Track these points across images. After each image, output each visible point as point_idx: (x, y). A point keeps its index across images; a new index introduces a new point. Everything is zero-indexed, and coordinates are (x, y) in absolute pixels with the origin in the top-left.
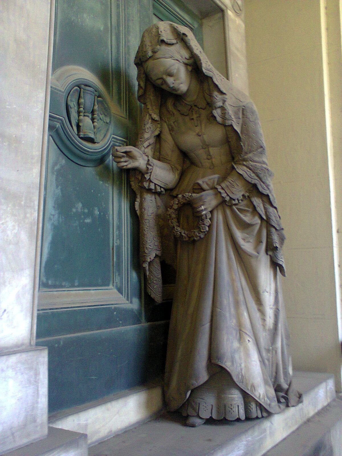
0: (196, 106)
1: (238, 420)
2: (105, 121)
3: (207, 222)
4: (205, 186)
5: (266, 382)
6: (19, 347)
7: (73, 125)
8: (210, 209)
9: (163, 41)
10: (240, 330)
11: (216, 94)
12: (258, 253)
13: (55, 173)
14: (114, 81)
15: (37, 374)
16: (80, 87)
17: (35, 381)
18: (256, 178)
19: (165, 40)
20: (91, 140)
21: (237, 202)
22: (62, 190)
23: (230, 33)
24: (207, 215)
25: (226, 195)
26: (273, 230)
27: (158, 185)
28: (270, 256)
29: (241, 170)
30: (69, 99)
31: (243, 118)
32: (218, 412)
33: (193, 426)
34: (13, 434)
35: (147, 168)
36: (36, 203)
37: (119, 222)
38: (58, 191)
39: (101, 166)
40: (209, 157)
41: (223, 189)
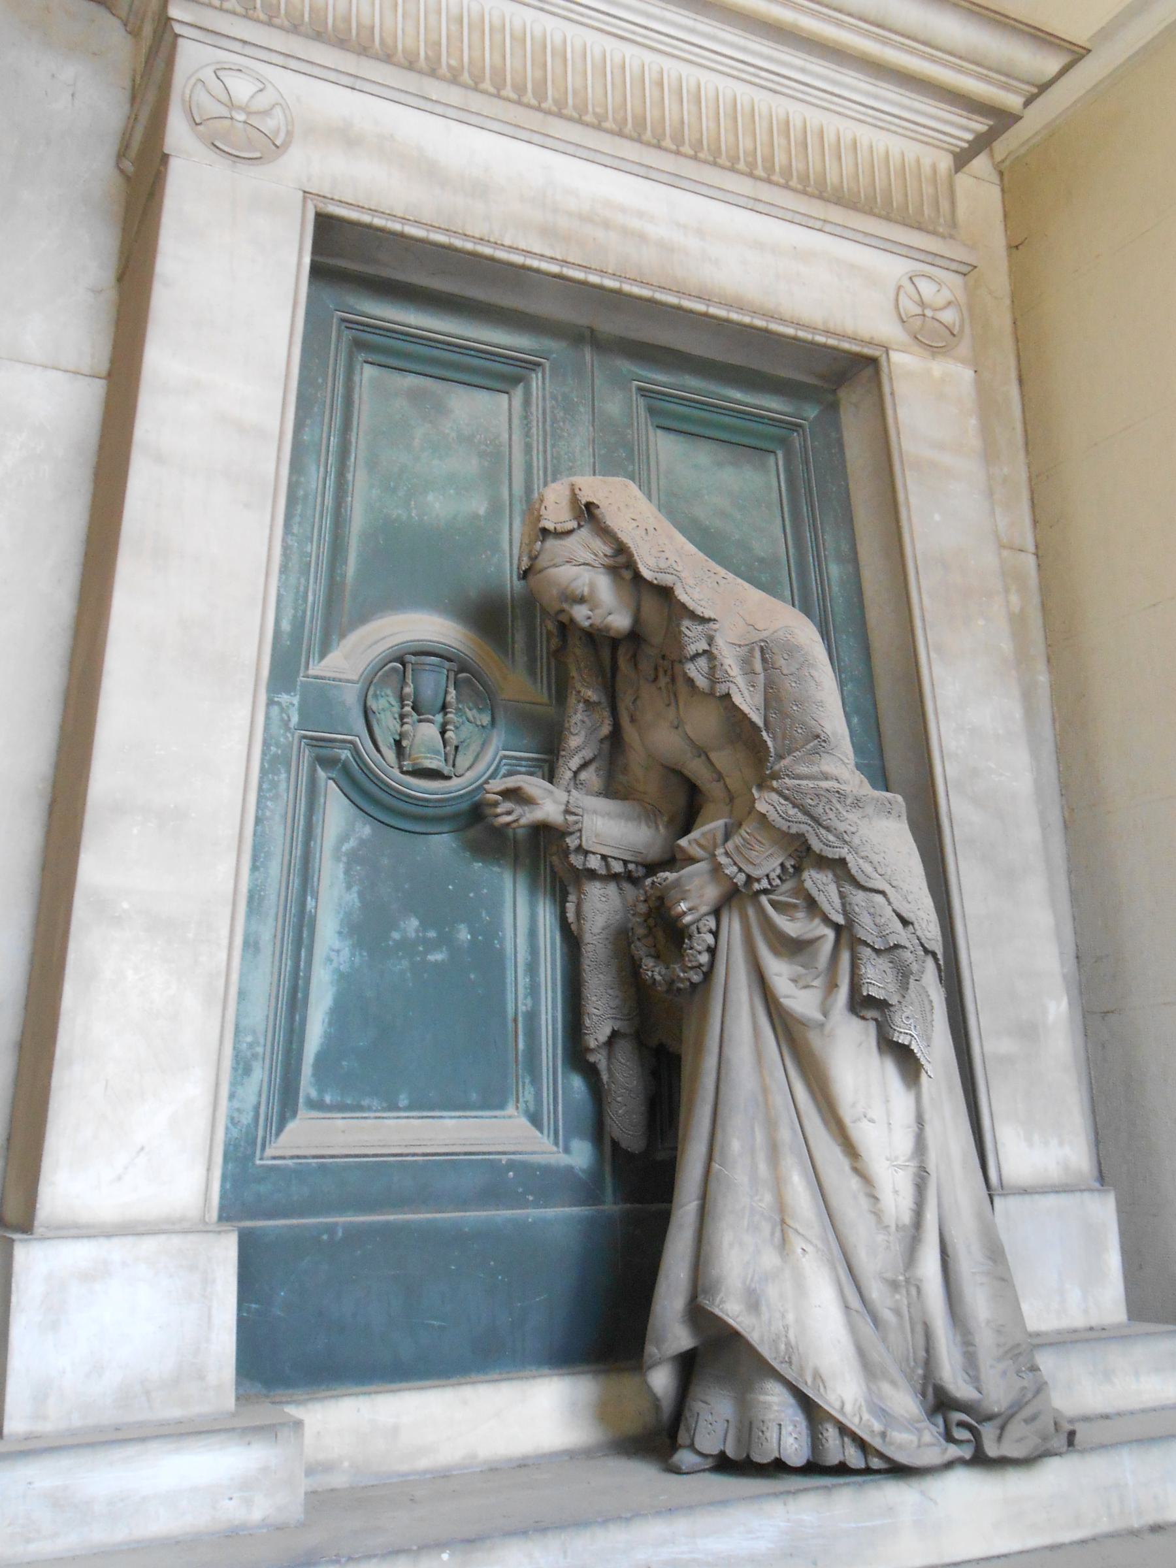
1: (779, 1468)
2: (479, 723)
4: (696, 851)
5: (869, 1369)
6: (173, 1223)
7: (383, 749)
8: (704, 909)
9: (545, 532)
10: (783, 1222)
11: (686, 623)
13: (344, 859)
14: (519, 623)
16: (404, 662)
19: (550, 526)
22: (361, 894)
23: (902, 413)
24: (701, 924)
25: (735, 869)
28: (876, 1020)
29: (765, 803)
30: (371, 693)
31: (765, 670)
32: (739, 1441)
33: (676, 1471)
34: (147, 1393)
36: (225, 932)
38: (353, 897)
39: (479, 827)
41: (727, 854)
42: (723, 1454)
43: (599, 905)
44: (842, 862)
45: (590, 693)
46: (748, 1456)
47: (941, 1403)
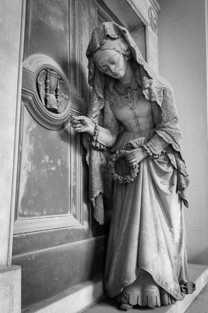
0: (129, 88)
3: (136, 171)
4: (135, 145)
8: (138, 162)
10: (158, 245)
12: (171, 192)
13: (29, 134)
15: (12, 288)
17: (11, 294)
18: (172, 140)
20: (55, 111)
21: (157, 156)
25: (150, 151)
26: (182, 176)
27: (102, 145)
29: (161, 134)
32: (142, 301)
33: (125, 310)
35: (95, 132)
37: (75, 169)
38: (31, 147)
39: (63, 130)
40: (138, 125)
41: (148, 147)
42: (137, 304)
43: (96, 157)
44: (179, 153)
45: (101, 95)
46: (147, 305)
47: (181, 282)
